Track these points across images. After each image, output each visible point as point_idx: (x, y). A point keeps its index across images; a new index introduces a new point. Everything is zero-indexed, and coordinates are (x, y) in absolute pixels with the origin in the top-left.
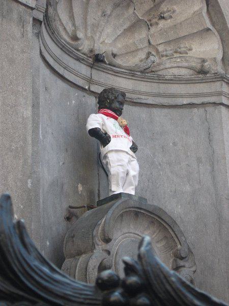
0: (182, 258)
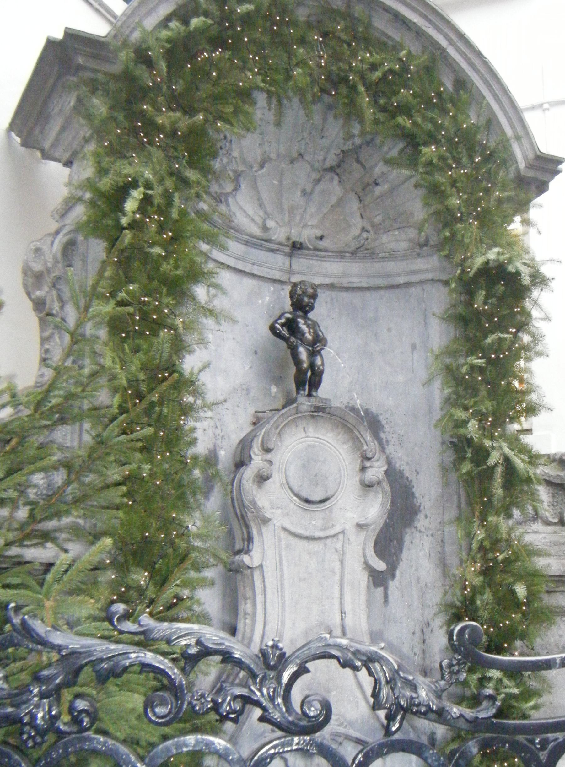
0: (369, 459)
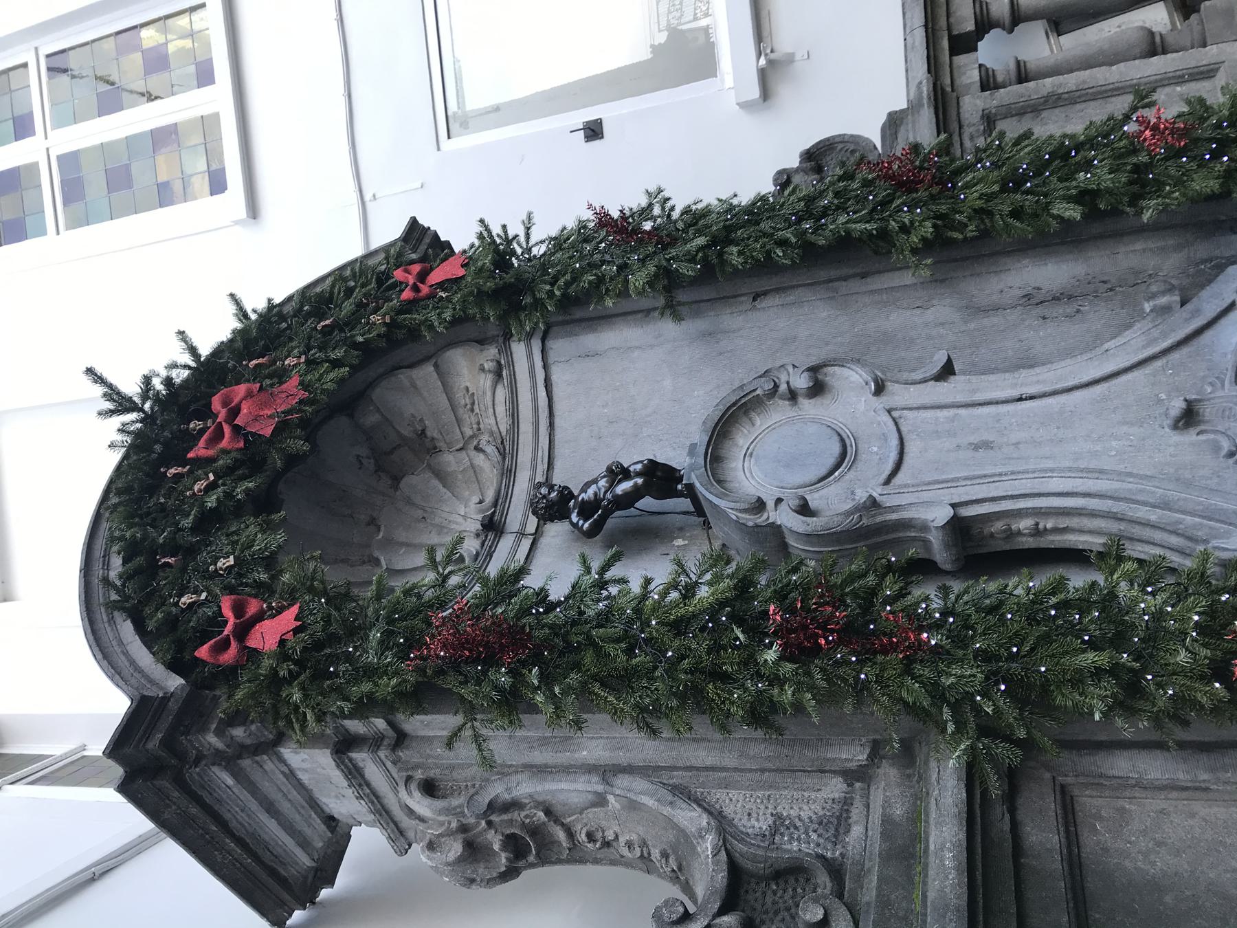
0: (776, 386)
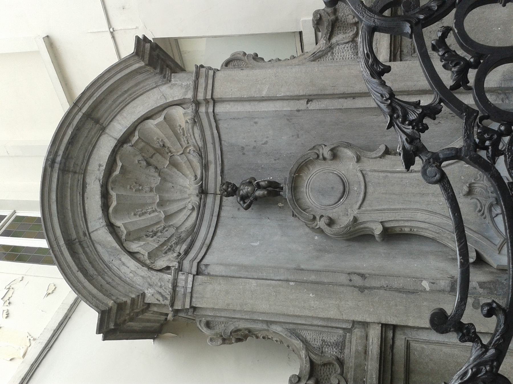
0: (318, 156)
